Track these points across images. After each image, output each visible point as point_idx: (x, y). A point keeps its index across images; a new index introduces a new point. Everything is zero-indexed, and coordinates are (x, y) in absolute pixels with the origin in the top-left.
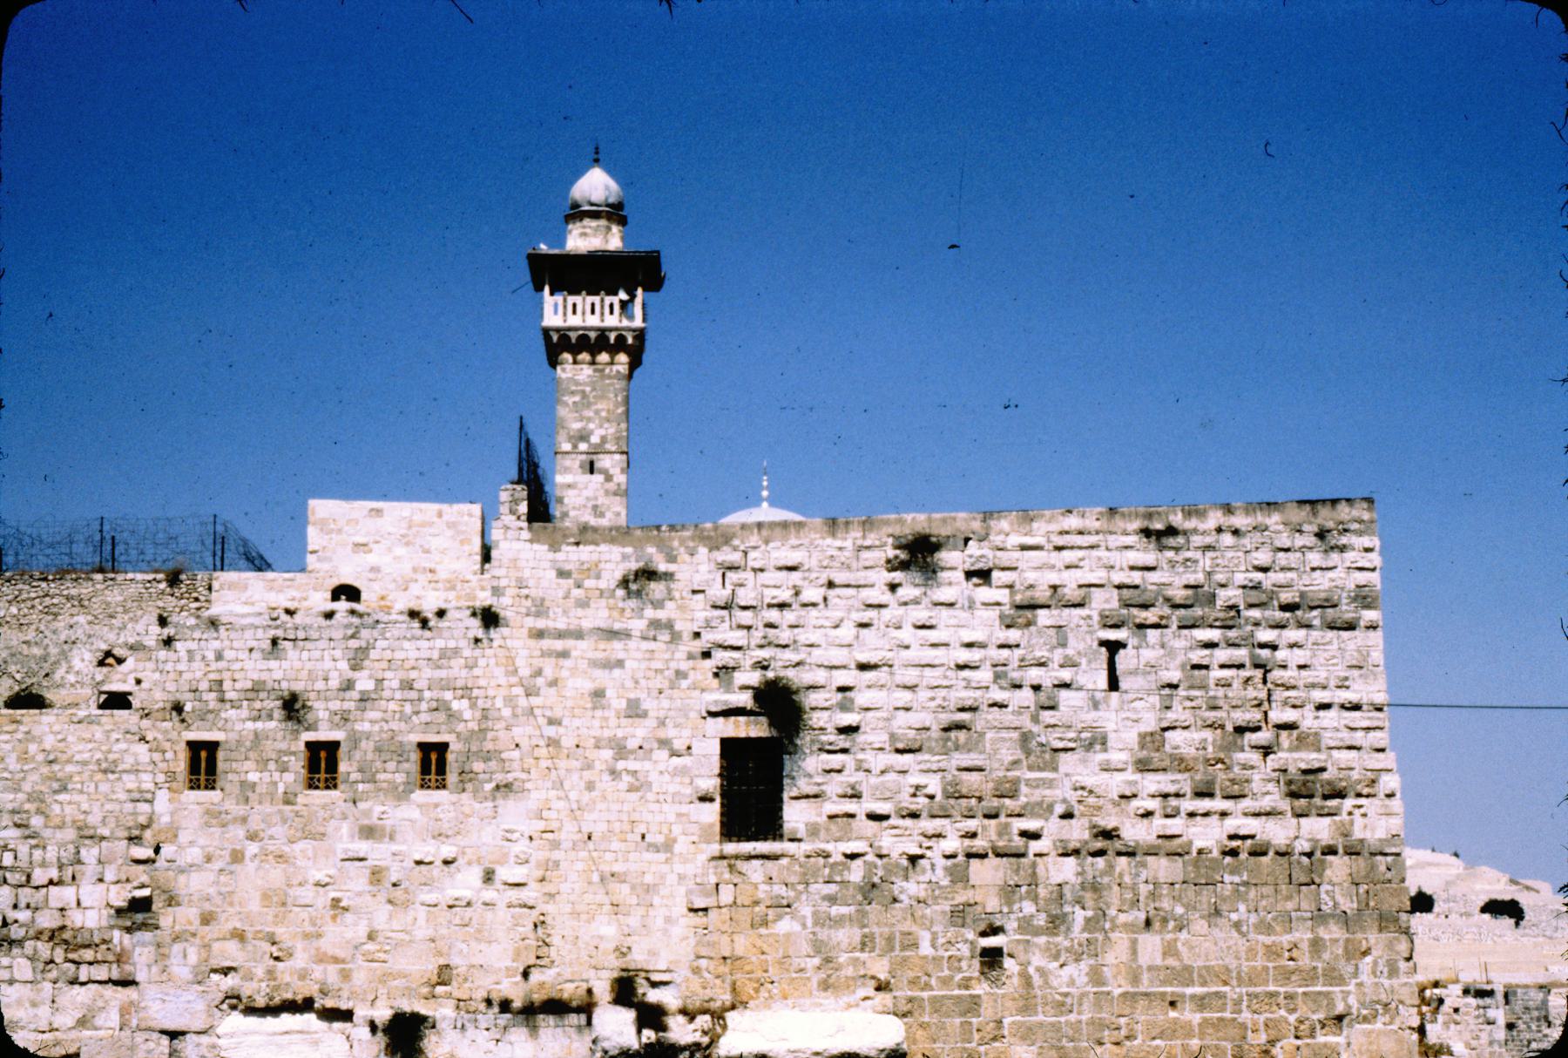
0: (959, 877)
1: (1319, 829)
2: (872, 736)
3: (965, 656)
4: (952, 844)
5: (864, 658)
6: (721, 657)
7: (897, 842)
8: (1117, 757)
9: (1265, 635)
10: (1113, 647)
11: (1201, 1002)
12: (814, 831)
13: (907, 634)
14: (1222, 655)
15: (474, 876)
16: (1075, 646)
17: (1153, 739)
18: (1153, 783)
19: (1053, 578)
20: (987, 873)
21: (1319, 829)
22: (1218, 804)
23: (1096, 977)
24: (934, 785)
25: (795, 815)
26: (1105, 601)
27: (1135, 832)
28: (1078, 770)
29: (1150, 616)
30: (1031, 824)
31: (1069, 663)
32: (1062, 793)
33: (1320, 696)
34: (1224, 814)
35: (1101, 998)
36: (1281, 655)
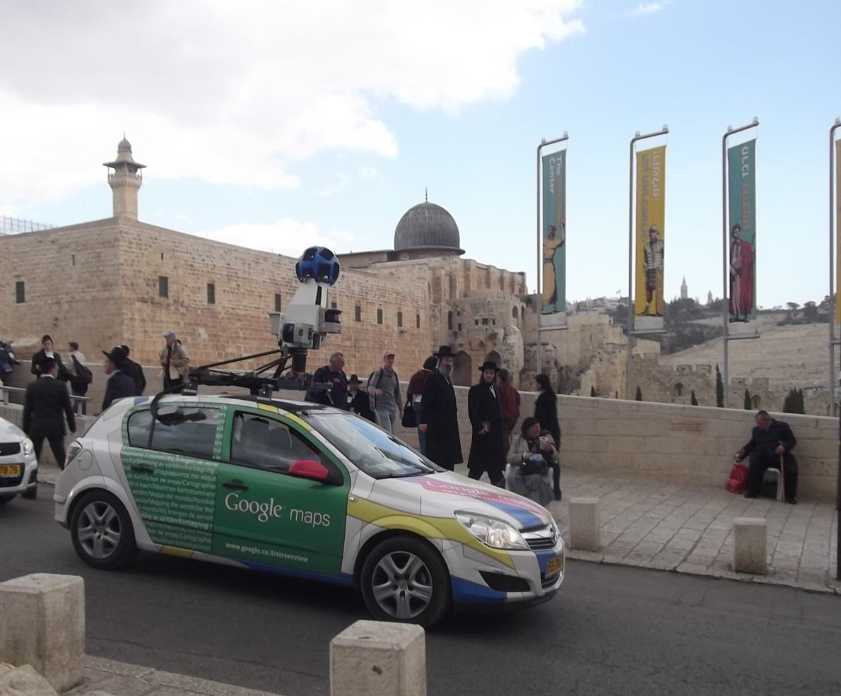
1: (107, 294)
3: (50, 260)
4: (49, 302)
5: (35, 262)
6: (15, 264)
8: (74, 280)
9: (98, 251)
10: (73, 256)
13: (42, 257)
14: (91, 256)
18: (80, 286)
19: (64, 241)
21: (107, 294)
22: (91, 290)
24: (46, 289)
25: (27, 297)
27: (78, 297)
29: (80, 248)
30: (60, 297)
31: (67, 261)
33: (107, 263)
34: (91, 292)
36: (102, 255)
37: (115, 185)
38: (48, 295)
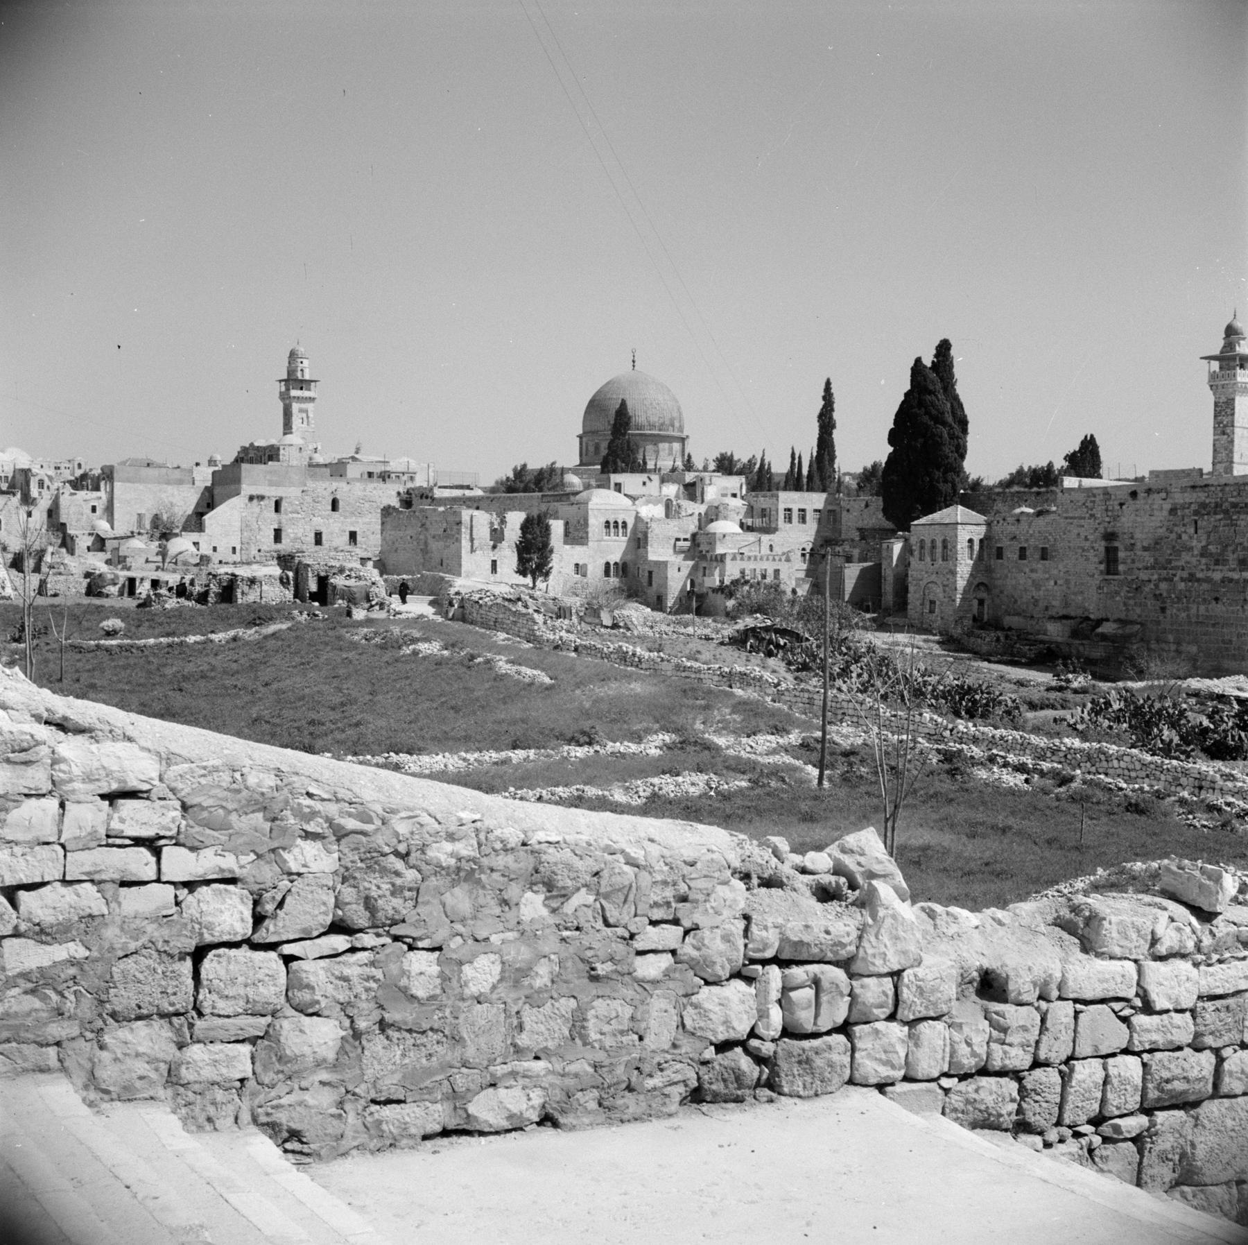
0: (1157, 586)
2: (1139, 545)
7: (1143, 576)
11: (1214, 625)
12: (1125, 573)
15: (1052, 583)
16: (1186, 520)
17: (1205, 548)
18: (1204, 561)
20: (1164, 586)
23: (1188, 616)
25: (1121, 568)
26: (1194, 507)
28: (1186, 557)
32: (1181, 563)
35: (1190, 623)
37: (1215, 382)
38: (1153, 568)
